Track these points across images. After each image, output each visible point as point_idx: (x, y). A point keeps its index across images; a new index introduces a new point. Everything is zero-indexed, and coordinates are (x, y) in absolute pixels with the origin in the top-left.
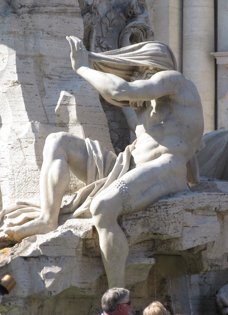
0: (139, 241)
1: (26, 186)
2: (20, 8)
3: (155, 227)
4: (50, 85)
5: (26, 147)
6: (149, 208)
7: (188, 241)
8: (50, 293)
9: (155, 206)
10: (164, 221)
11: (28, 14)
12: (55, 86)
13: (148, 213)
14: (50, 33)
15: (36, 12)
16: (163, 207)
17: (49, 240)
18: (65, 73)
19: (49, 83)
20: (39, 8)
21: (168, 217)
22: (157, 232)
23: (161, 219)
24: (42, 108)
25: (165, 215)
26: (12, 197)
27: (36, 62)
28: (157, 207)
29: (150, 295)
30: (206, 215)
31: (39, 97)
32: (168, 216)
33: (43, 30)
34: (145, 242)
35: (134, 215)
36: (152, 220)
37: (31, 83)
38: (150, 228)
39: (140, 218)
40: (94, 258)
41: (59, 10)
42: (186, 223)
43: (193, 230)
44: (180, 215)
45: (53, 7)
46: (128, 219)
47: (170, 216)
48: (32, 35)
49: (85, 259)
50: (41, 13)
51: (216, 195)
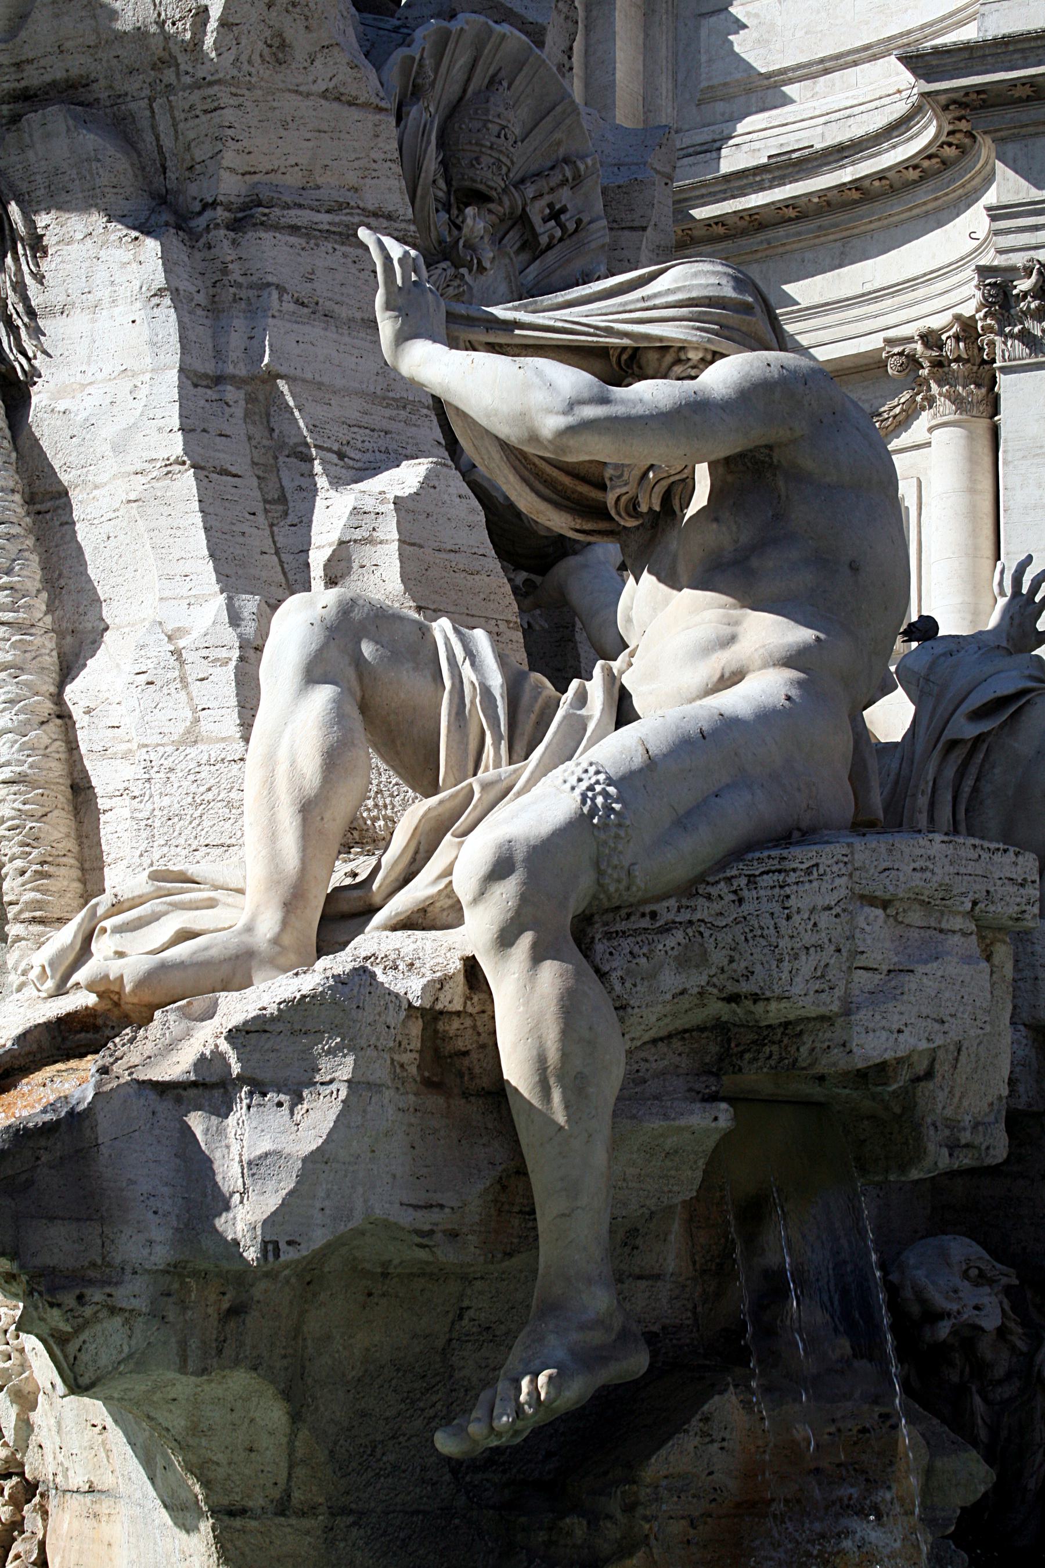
0: (663, 1033)
1: (197, 822)
2: (200, 214)
3: (734, 965)
5: (202, 680)
6: (708, 883)
7: (874, 1031)
8: (270, 1247)
9: (732, 877)
10: (773, 940)
11: (227, 233)
13: (704, 910)
14: (306, 301)
15: (254, 225)
16: (767, 880)
17: (272, 1009)
18: (359, 445)
19: (302, 475)
20: (267, 211)
22: (745, 987)
23: (759, 933)
24: (275, 558)
25: (776, 915)
26: (141, 865)
27: (250, 399)
28: (743, 881)
29: (698, 1267)
30: (935, 929)
31: (261, 518)
32: (788, 918)
33: (281, 289)
34: (687, 1035)
35: (643, 915)
36: (720, 936)
37: (233, 470)
38: (712, 974)
39: (666, 929)
40: (473, 1099)
41: (338, 224)
42: (863, 952)
43: (893, 983)
44: (837, 916)
45: (319, 211)
46: (617, 932)
47: (796, 918)
48: (243, 305)
49: (435, 1101)
50: (276, 227)
51: (975, 846)
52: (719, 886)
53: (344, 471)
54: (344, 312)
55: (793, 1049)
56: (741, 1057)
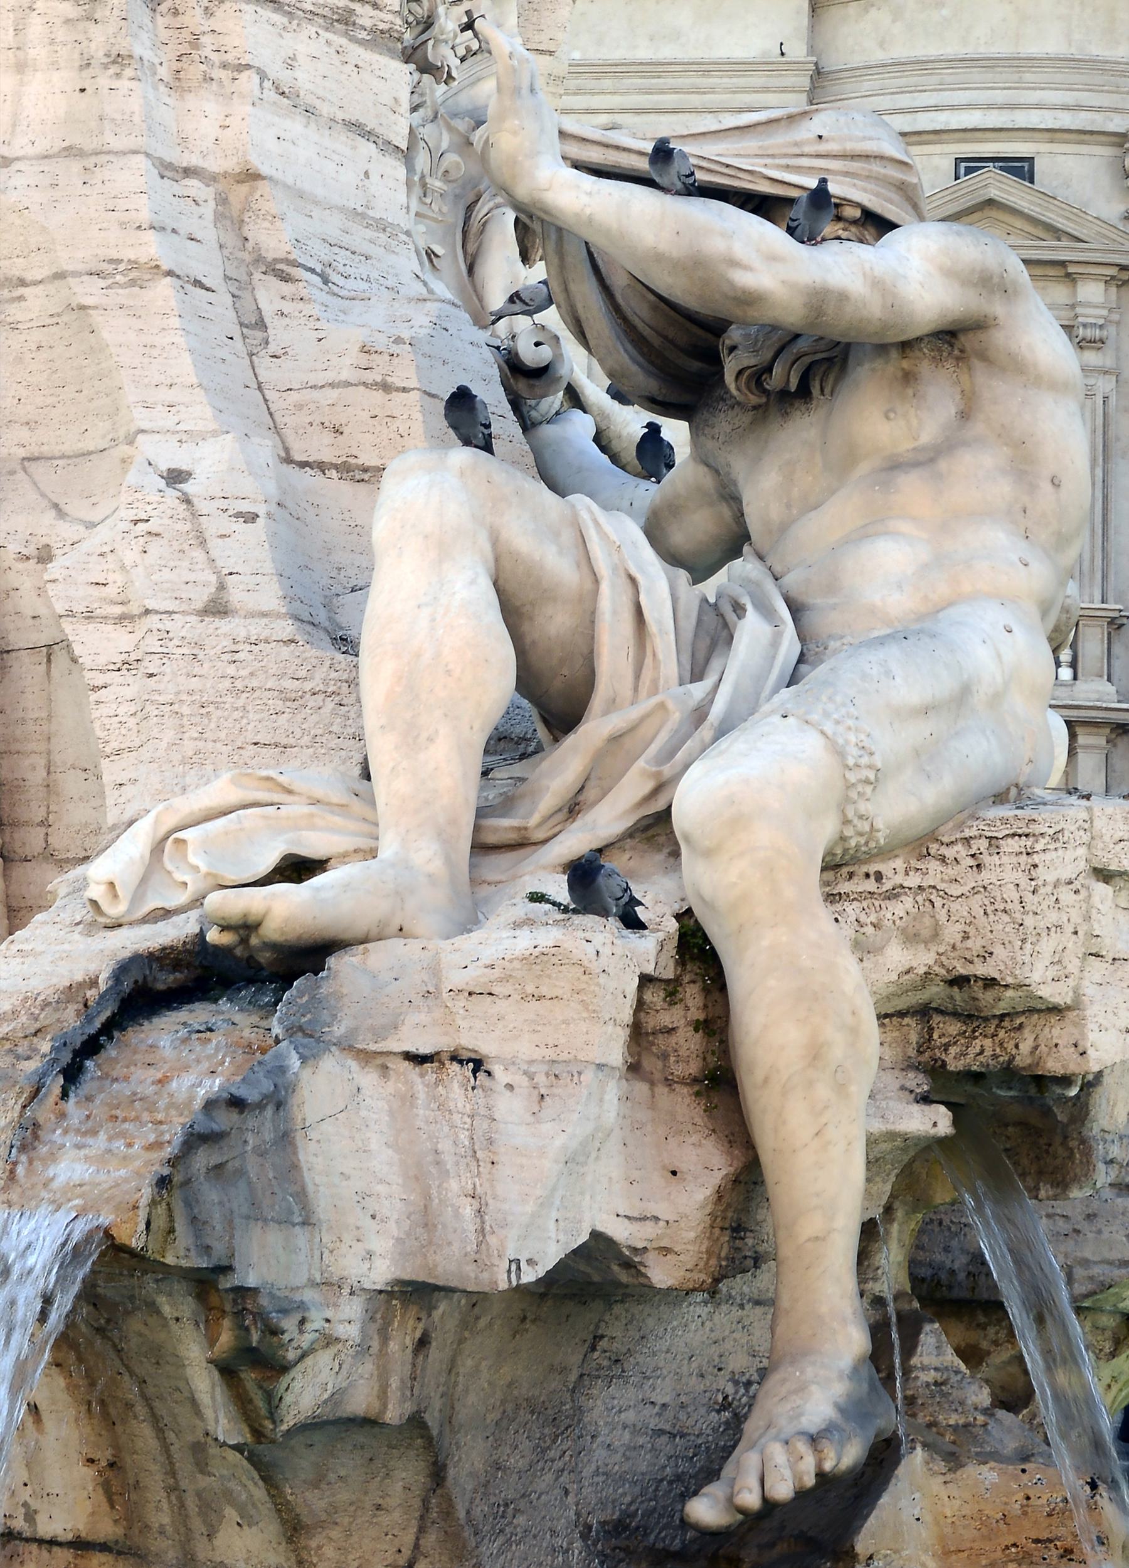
3: (969, 943)
4: (287, 307)
10: (1018, 916)
12: (308, 309)
14: (287, 91)
16: (1013, 845)
18: (341, 269)
21: (1036, 899)
22: (981, 969)
25: (1021, 887)
27: (222, 200)
28: (983, 844)
35: (867, 876)
36: (955, 906)
37: (206, 282)
38: (941, 951)
39: (893, 895)
43: (1120, 974)
44: (1076, 892)
47: (1042, 891)
52: (956, 848)
53: (329, 297)
54: (325, 109)
55: (1010, 1046)
56: (946, 1050)
